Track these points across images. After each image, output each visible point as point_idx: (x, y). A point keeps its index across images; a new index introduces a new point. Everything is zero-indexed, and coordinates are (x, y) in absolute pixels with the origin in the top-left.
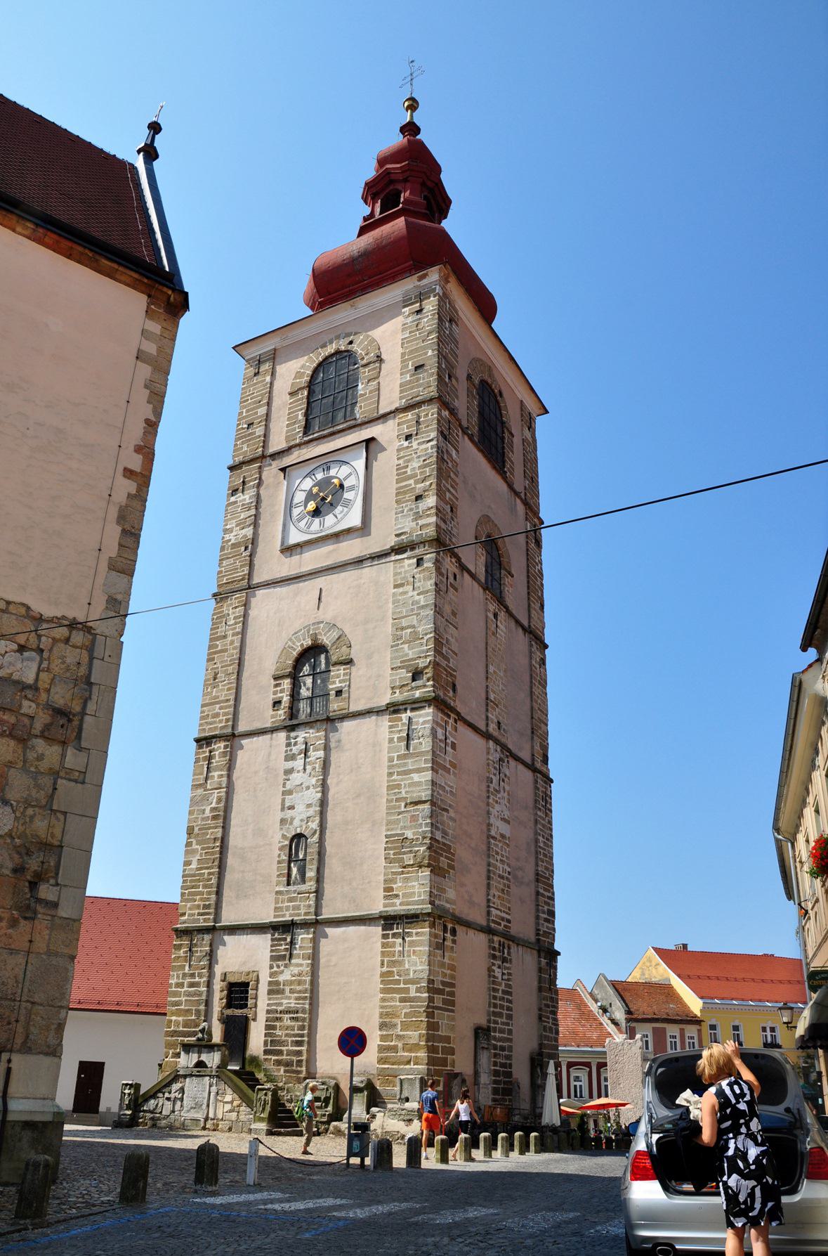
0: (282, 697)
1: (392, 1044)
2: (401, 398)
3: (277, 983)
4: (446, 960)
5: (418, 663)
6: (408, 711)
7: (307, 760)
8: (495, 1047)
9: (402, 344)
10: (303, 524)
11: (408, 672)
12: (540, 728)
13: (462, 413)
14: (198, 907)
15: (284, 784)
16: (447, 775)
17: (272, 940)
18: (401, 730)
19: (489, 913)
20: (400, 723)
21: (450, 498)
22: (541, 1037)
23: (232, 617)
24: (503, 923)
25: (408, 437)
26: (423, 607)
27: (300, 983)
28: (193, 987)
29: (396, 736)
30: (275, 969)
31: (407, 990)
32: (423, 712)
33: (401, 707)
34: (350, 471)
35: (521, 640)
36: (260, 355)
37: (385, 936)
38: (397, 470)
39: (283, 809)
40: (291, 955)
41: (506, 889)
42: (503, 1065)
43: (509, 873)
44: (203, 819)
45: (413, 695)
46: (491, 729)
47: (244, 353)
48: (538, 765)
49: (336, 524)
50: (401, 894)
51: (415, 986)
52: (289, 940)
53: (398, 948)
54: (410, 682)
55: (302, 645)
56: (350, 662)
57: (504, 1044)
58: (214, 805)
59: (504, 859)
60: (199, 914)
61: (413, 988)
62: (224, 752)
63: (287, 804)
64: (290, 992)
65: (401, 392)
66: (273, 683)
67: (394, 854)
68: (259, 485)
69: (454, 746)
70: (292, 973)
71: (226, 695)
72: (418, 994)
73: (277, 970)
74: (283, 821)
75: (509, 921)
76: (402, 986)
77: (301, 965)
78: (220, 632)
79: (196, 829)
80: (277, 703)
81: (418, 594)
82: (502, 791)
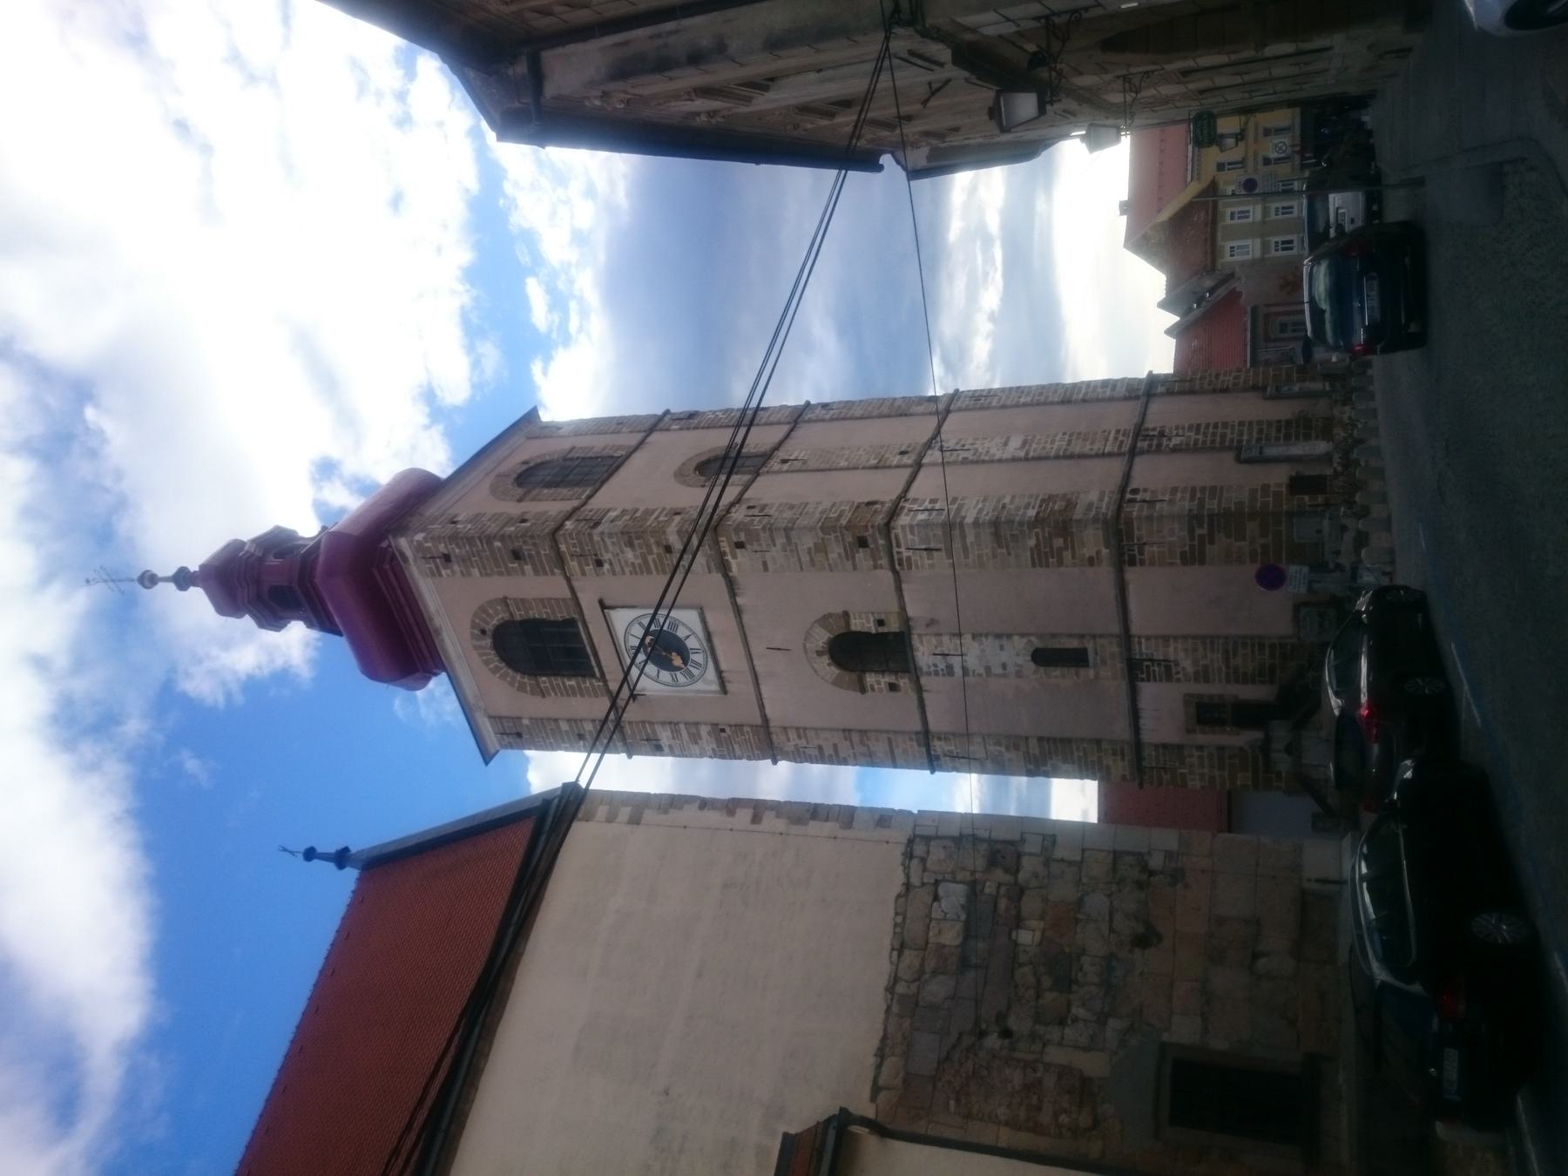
0: (885, 682)
1: (1259, 550)
2: (553, 574)
3: (1196, 673)
4: (1167, 498)
5: (849, 543)
6: (900, 550)
7: (952, 653)
8: (1259, 440)
9: (487, 575)
10: (695, 672)
11: (858, 553)
12: (899, 407)
13: (568, 506)
15: (980, 675)
16: (966, 507)
17: (1149, 680)
18: (921, 557)
19: (1110, 455)
21: (666, 516)
22: (1244, 390)
23: (798, 742)
24: (1121, 438)
25: (599, 563)
27: (1195, 650)
29: (927, 562)
30: (1180, 676)
31: (1201, 537)
32: (901, 536)
33: (896, 558)
34: (637, 625)
35: (803, 432)
36: (495, 733)
37: (1142, 563)
38: (636, 573)
39: (1005, 676)
40: (1164, 661)
41: (1082, 436)
42: (1279, 431)
43: (1064, 434)
45: (883, 545)
46: (910, 462)
47: (493, 751)
48: (941, 406)
49: (697, 637)
51: (1197, 529)
53: (1155, 548)
54: (868, 550)
55: (829, 665)
56: (846, 615)
57: (1255, 430)
58: (1003, 749)
59: (1049, 440)
61: (1199, 532)
65: (546, 574)
66: (869, 693)
68: (651, 723)
69: (933, 501)
72: (1206, 526)
75: (1118, 431)
76: (1196, 543)
77: (1175, 649)
78: (815, 752)
80: (893, 687)
81: (775, 545)
82: (975, 446)
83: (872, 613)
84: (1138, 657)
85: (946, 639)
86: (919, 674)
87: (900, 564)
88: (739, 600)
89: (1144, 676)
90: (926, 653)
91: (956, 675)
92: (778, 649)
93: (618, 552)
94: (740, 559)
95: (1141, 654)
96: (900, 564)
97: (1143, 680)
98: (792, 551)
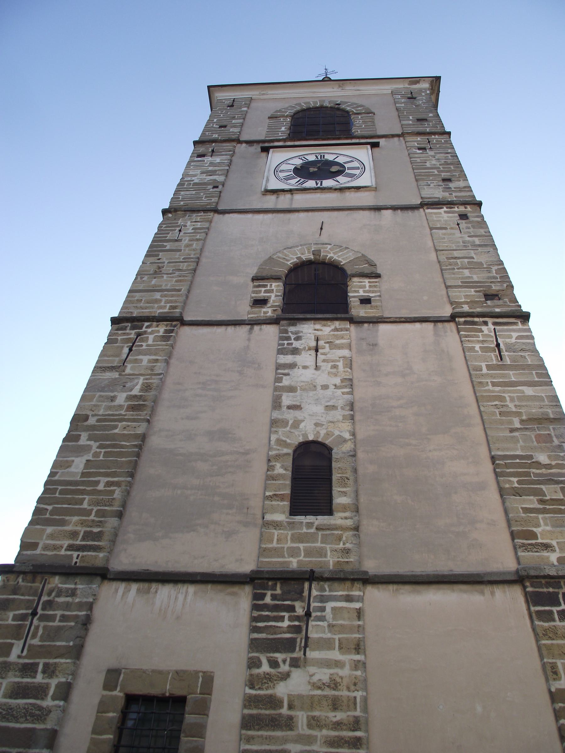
7: (321, 357)
14: (74, 535)
15: (278, 380)
17: (255, 607)
20: (480, 334)
26: (480, 246)
27: (335, 705)
28: (24, 697)
30: (265, 668)
32: (514, 327)
33: (476, 319)
39: (277, 404)
40: (307, 638)
44: (110, 408)
50: (554, 543)
52: (300, 611)
56: (378, 276)
60: (71, 548)
62: (163, 336)
63: (287, 400)
64: (310, 726)
66: (251, 284)
67: (518, 482)
70: (315, 679)
71: (173, 285)
73: (273, 671)
74: (274, 423)
77: (338, 664)
79: (92, 421)
83: (380, 296)
84: (314, 593)
85: (345, 353)
86: (282, 322)
87: (465, 321)
88: (387, 213)
89: (268, 600)
90: (318, 333)
91: (282, 356)
92: (321, 229)
93: (437, 158)
94: (445, 215)
95: (323, 599)
96: (466, 323)
97: (258, 597)
98: (465, 246)
